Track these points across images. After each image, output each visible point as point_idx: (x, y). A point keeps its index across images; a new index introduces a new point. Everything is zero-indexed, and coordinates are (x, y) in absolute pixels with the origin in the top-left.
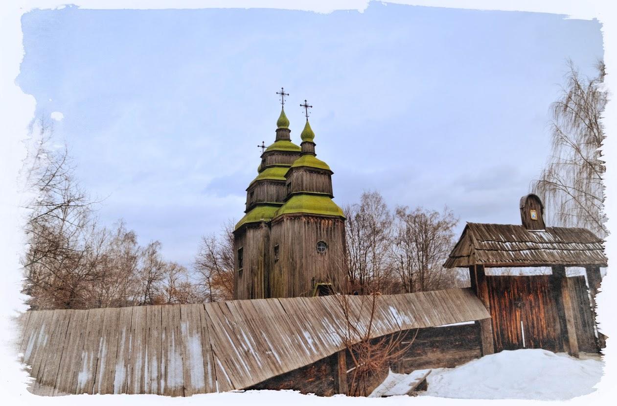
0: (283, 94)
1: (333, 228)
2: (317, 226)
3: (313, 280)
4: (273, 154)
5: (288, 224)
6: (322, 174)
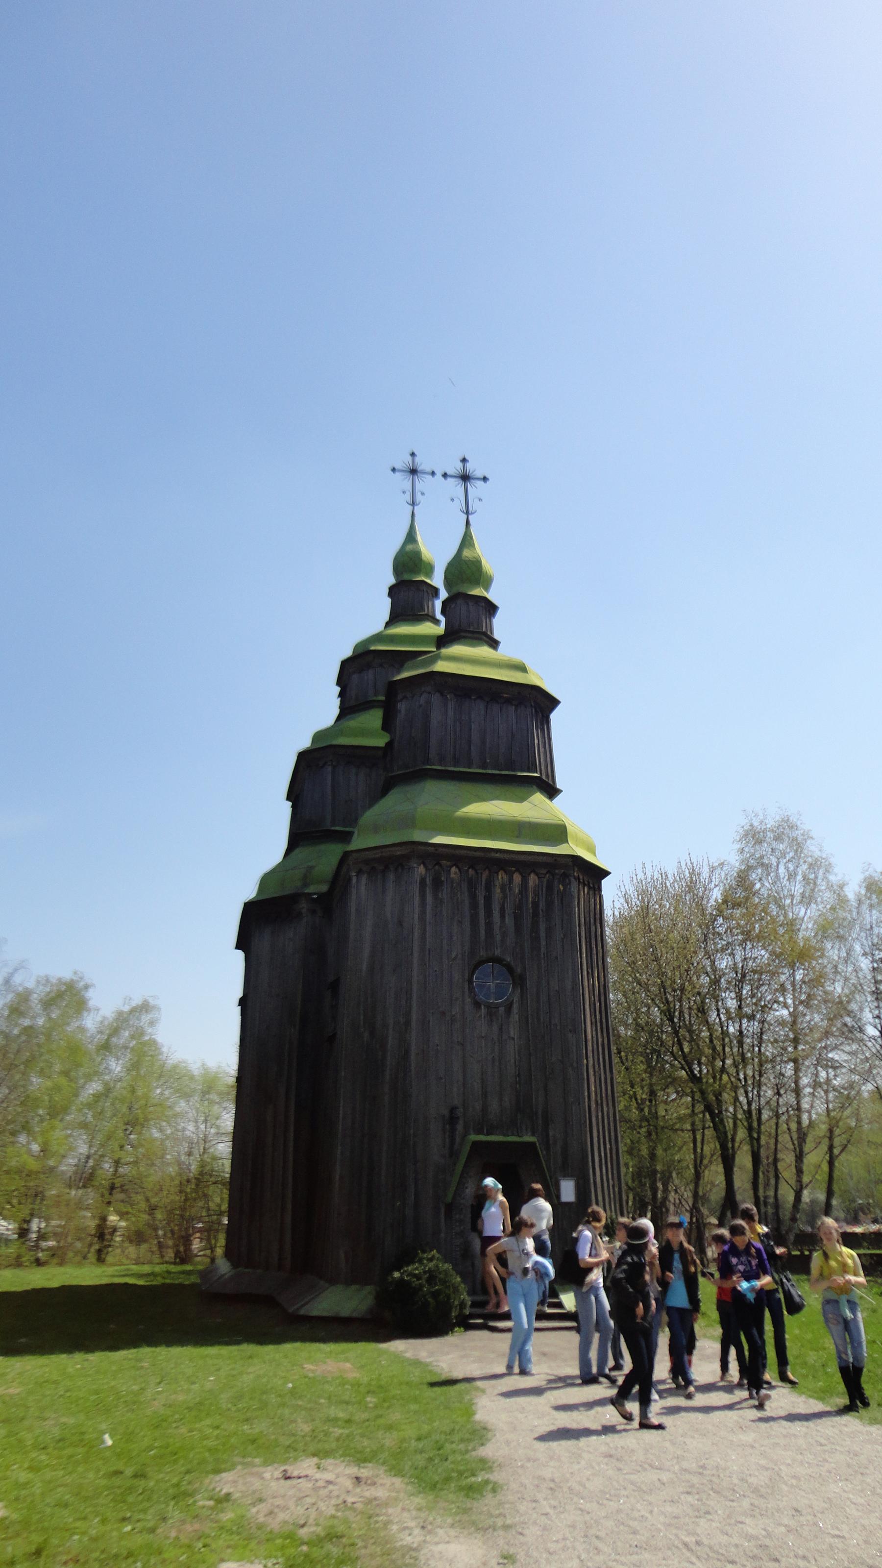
0: (413, 471)
1: (542, 905)
2: (473, 897)
3: (452, 1119)
4: (369, 666)
5: (363, 888)
6: (508, 701)
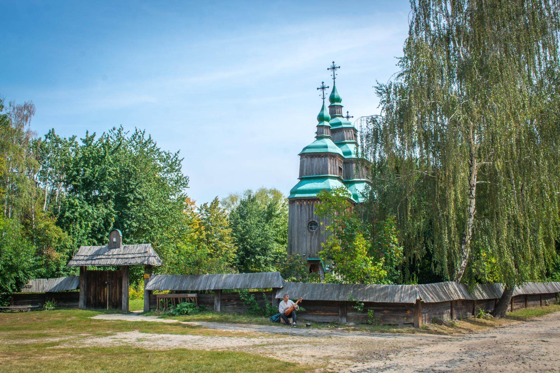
0: (334, 68)
2: (309, 208)
6: (323, 157)
